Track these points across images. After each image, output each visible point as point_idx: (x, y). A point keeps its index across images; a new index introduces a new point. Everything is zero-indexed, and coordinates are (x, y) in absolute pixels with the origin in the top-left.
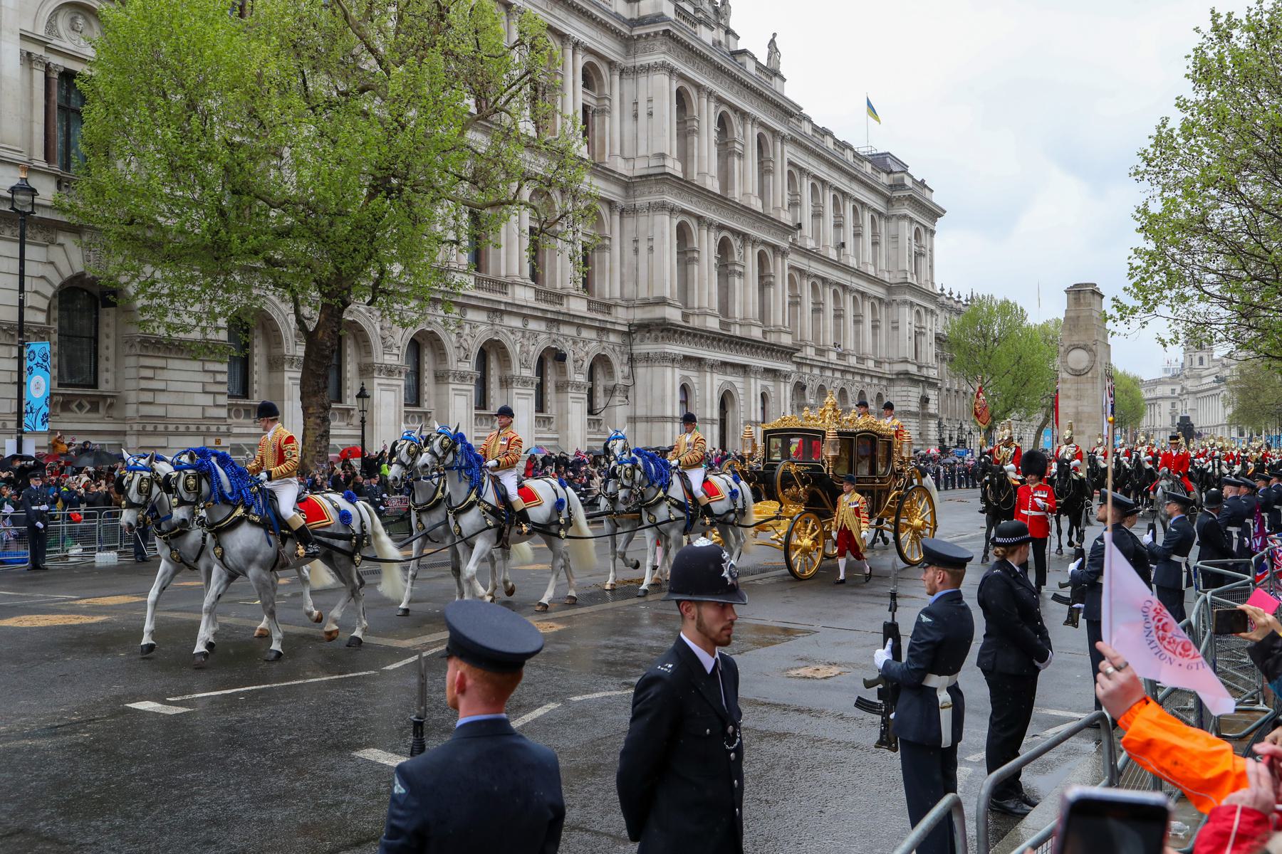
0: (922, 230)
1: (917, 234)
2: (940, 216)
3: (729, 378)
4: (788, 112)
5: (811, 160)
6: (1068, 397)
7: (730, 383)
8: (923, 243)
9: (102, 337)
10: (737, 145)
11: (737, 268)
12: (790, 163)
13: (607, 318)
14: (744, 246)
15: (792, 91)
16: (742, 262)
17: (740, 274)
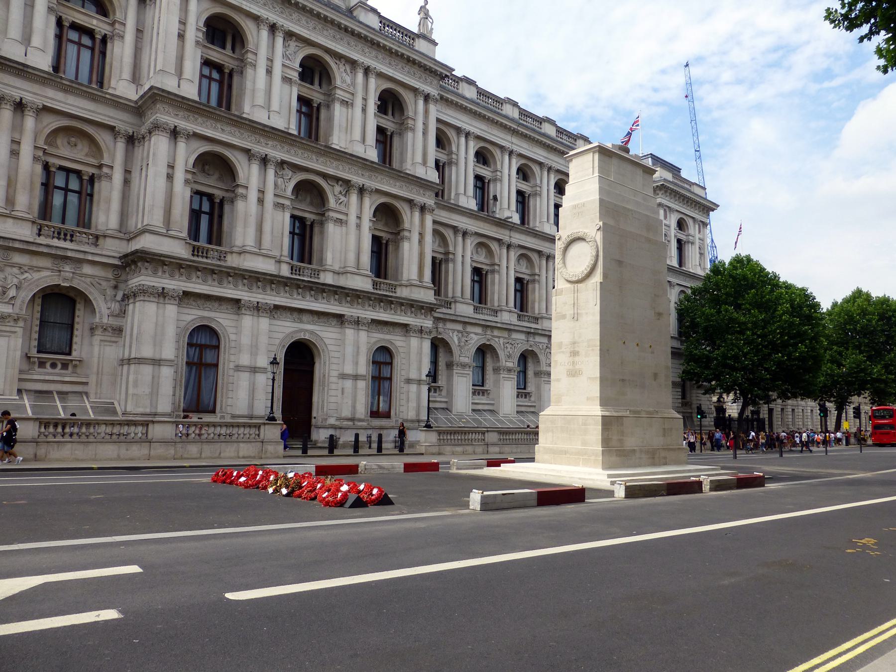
0: (690, 222)
1: (681, 225)
2: (713, 210)
3: (206, 314)
4: (441, 74)
5: (515, 140)
6: (564, 317)
7: (312, 332)
8: (691, 231)
9: (76, 326)
10: (338, 92)
11: (331, 214)
12: (439, 120)
13: (449, 311)
14: (347, 193)
15: (442, 55)
16: (342, 208)
17: (340, 222)
